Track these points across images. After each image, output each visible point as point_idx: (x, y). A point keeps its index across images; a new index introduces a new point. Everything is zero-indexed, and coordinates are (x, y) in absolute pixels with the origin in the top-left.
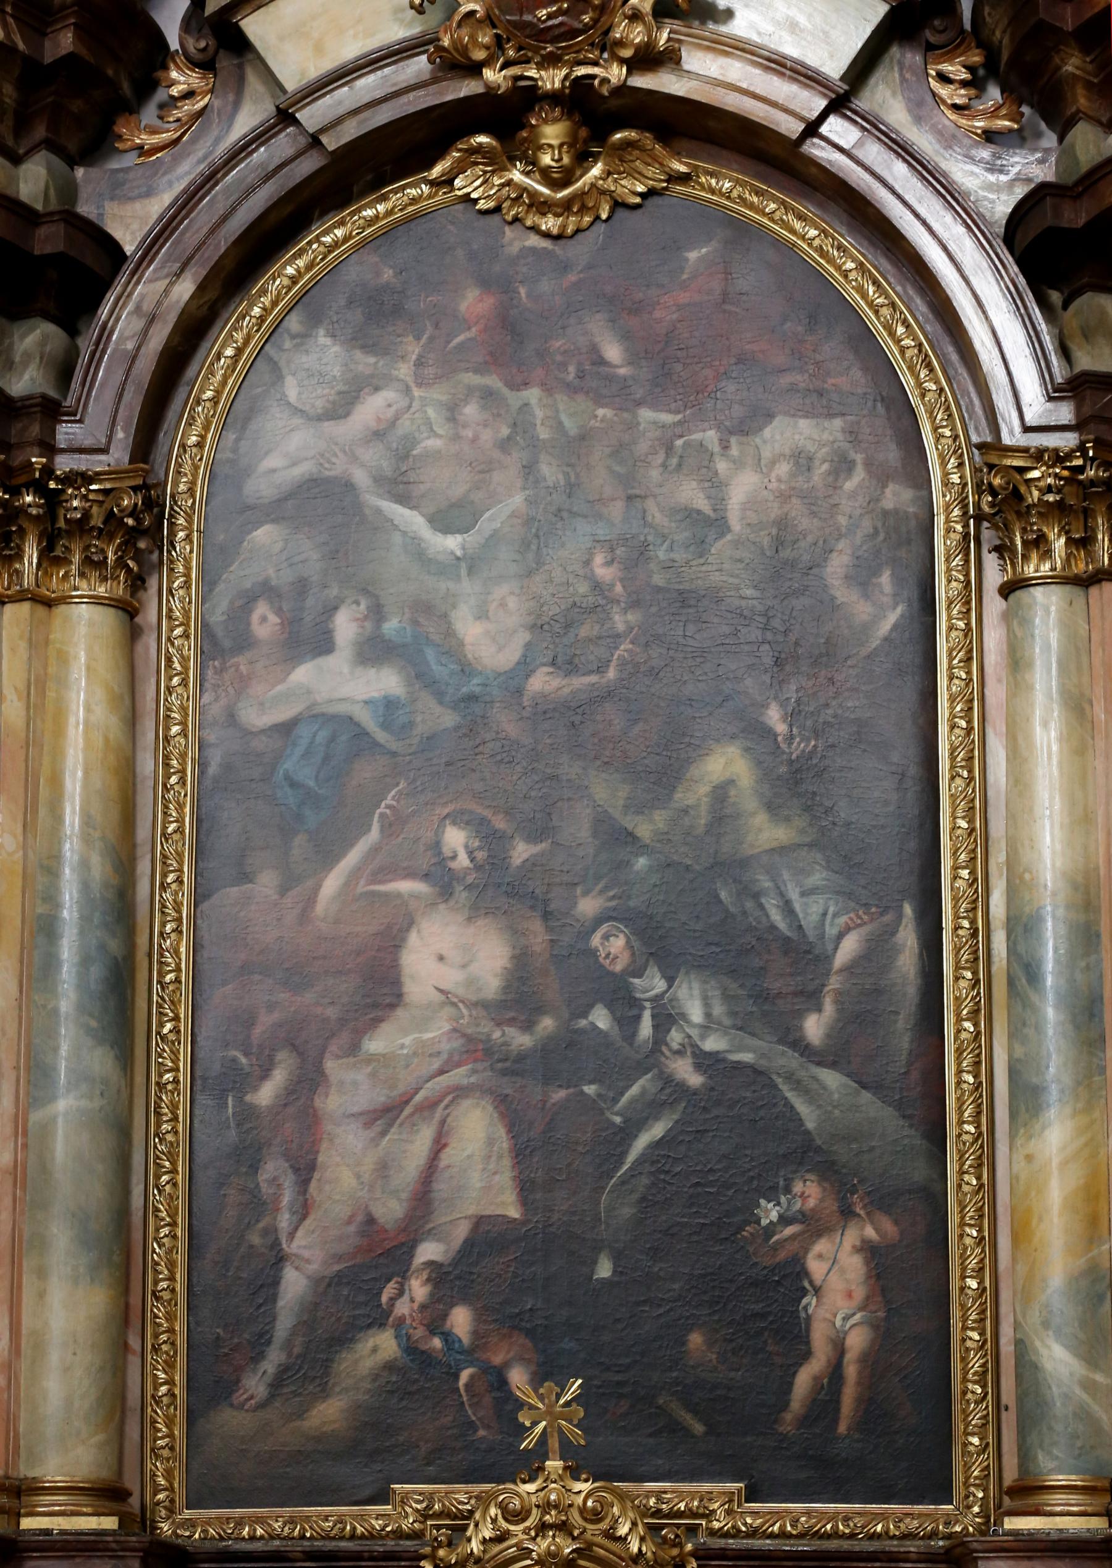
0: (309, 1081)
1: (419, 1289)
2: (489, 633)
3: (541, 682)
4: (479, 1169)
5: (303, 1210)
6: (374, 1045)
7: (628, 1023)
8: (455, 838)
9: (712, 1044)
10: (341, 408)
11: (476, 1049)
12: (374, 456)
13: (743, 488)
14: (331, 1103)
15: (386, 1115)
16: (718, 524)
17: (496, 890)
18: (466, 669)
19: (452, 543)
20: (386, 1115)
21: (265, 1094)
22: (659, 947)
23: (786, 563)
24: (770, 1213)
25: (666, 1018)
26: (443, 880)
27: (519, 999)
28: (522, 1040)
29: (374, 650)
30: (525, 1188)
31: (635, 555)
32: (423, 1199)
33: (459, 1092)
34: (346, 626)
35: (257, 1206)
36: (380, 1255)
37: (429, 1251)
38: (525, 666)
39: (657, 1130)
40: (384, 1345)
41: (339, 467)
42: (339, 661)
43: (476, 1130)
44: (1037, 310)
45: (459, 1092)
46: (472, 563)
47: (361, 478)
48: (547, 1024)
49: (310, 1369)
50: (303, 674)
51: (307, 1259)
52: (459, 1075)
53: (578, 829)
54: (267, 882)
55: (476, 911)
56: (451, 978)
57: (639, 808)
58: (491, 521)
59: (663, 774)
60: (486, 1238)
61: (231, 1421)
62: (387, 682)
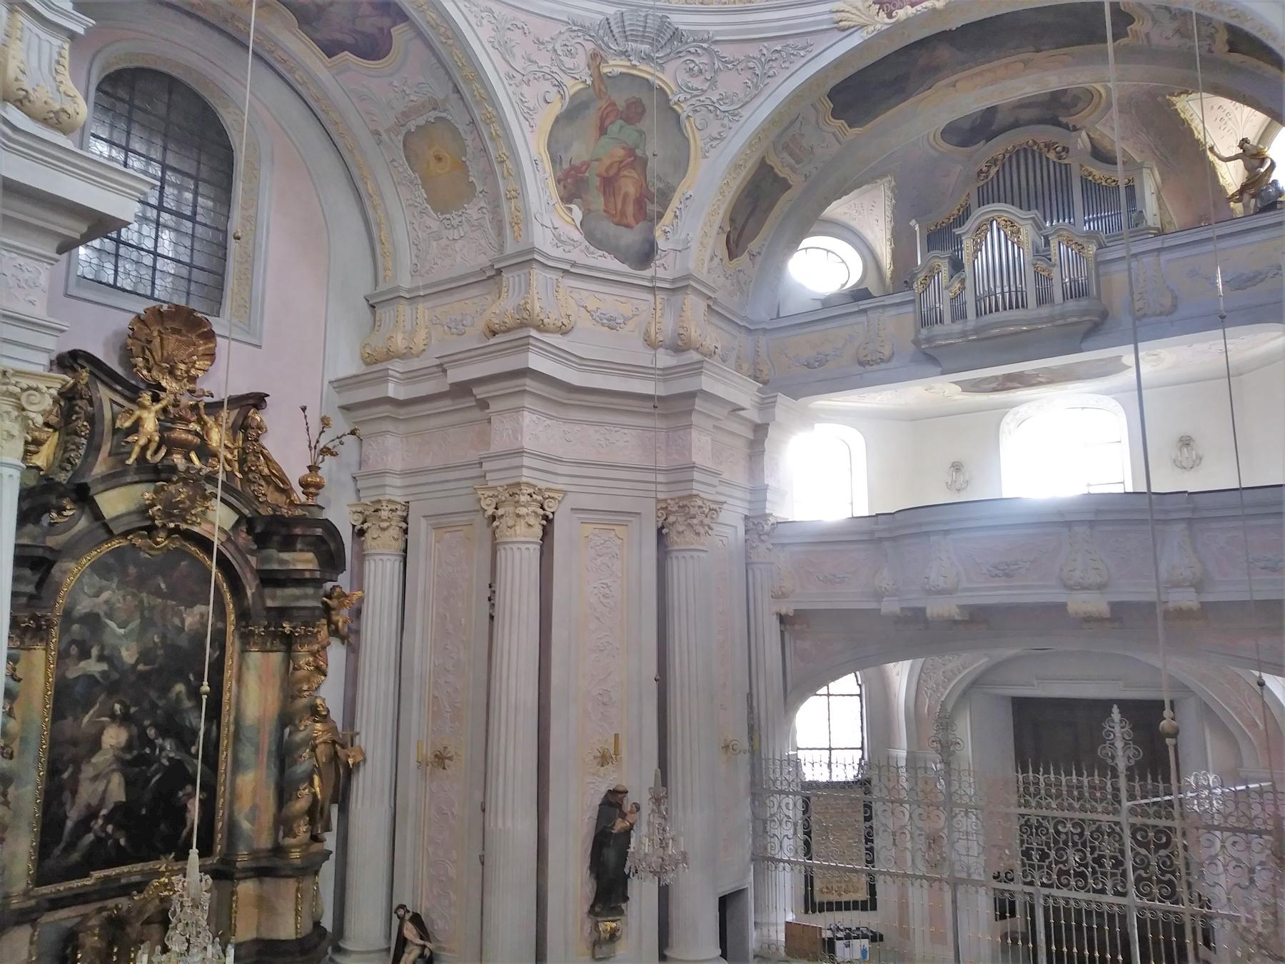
0: (78, 771)
1: (100, 822)
2: (128, 655)
3: (141, 667)
4: (117, 790)
5: (73, 803)
6: (94, 760)
7: (153, 750)
8: (117, 707)
9: (172, 755)
10: (97, 595)
11: (118, 759)
12: (105, 608)
13: (189, 621)
14: (82, 776)
15: (95, 778)
16: (183, 629)
17: (125, 719)
18: (123, 663)
19: (122, 631)
20: (95, 778)
21: (65, 775)
22: (164, 732)
23: (197, 640)
24: (181, 794)
25: (162, 749)
26: (113, 716)
27: (129, 747)
28: (128, 757)
29: (101, 658)
30: (127, 795)
31: (164, 637)
32: (103, 800)
33: (113, 771)
34: (95, 652)
35: (62, 804)
36: (92, 814)
37: (104, 812)
38: (137, 662)
39: (158, 777)
40: (90, 837)
41: (96, 610)
42: (92, 661)
43: (117, 781)
44: (228, 596)
45: (113, 771)
46: (125, 636)
47: (102, 614)
48: (135, 752)
49: (71, 846)
50: (82, 664)
51: (73, 815)
52: (114, 766)
53: (146, 705)
54: (70, 719)
55: (121, 725)
56: (113, 742)
57: (160, 698)
58: (131, 626)
59: (165, 690)
60: (118, 806)
61: (50, 863)
62: (104, 667)
